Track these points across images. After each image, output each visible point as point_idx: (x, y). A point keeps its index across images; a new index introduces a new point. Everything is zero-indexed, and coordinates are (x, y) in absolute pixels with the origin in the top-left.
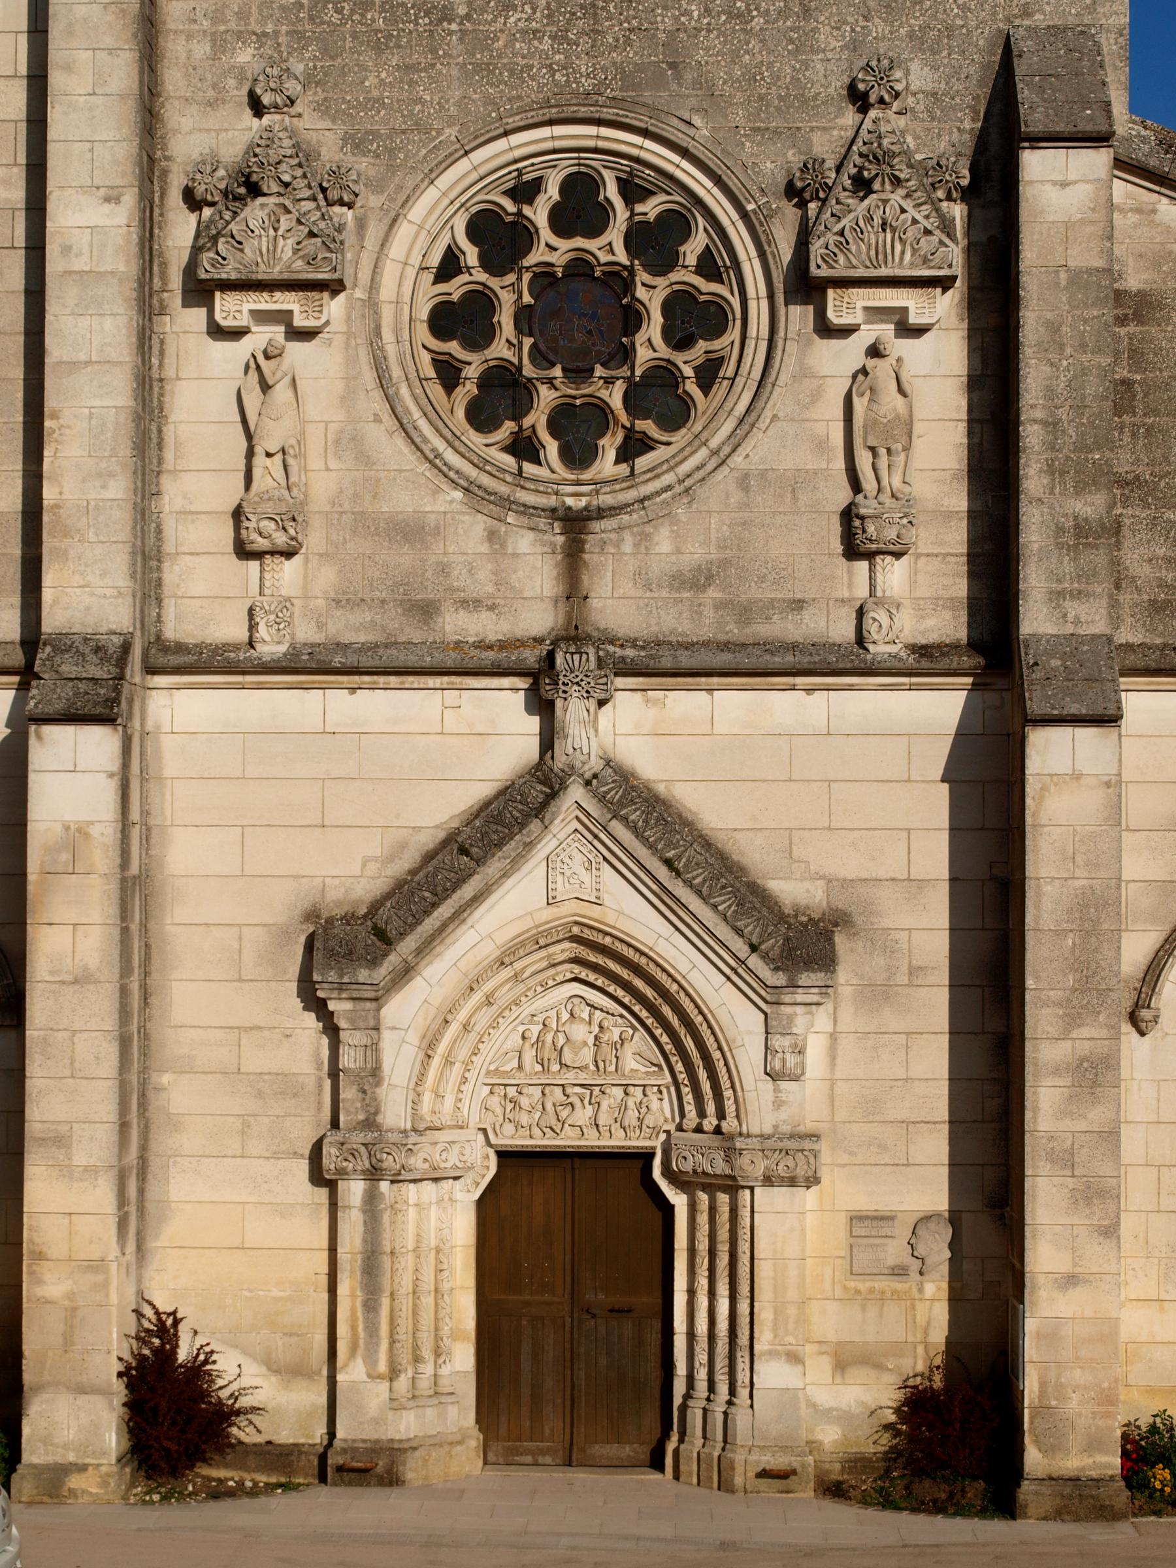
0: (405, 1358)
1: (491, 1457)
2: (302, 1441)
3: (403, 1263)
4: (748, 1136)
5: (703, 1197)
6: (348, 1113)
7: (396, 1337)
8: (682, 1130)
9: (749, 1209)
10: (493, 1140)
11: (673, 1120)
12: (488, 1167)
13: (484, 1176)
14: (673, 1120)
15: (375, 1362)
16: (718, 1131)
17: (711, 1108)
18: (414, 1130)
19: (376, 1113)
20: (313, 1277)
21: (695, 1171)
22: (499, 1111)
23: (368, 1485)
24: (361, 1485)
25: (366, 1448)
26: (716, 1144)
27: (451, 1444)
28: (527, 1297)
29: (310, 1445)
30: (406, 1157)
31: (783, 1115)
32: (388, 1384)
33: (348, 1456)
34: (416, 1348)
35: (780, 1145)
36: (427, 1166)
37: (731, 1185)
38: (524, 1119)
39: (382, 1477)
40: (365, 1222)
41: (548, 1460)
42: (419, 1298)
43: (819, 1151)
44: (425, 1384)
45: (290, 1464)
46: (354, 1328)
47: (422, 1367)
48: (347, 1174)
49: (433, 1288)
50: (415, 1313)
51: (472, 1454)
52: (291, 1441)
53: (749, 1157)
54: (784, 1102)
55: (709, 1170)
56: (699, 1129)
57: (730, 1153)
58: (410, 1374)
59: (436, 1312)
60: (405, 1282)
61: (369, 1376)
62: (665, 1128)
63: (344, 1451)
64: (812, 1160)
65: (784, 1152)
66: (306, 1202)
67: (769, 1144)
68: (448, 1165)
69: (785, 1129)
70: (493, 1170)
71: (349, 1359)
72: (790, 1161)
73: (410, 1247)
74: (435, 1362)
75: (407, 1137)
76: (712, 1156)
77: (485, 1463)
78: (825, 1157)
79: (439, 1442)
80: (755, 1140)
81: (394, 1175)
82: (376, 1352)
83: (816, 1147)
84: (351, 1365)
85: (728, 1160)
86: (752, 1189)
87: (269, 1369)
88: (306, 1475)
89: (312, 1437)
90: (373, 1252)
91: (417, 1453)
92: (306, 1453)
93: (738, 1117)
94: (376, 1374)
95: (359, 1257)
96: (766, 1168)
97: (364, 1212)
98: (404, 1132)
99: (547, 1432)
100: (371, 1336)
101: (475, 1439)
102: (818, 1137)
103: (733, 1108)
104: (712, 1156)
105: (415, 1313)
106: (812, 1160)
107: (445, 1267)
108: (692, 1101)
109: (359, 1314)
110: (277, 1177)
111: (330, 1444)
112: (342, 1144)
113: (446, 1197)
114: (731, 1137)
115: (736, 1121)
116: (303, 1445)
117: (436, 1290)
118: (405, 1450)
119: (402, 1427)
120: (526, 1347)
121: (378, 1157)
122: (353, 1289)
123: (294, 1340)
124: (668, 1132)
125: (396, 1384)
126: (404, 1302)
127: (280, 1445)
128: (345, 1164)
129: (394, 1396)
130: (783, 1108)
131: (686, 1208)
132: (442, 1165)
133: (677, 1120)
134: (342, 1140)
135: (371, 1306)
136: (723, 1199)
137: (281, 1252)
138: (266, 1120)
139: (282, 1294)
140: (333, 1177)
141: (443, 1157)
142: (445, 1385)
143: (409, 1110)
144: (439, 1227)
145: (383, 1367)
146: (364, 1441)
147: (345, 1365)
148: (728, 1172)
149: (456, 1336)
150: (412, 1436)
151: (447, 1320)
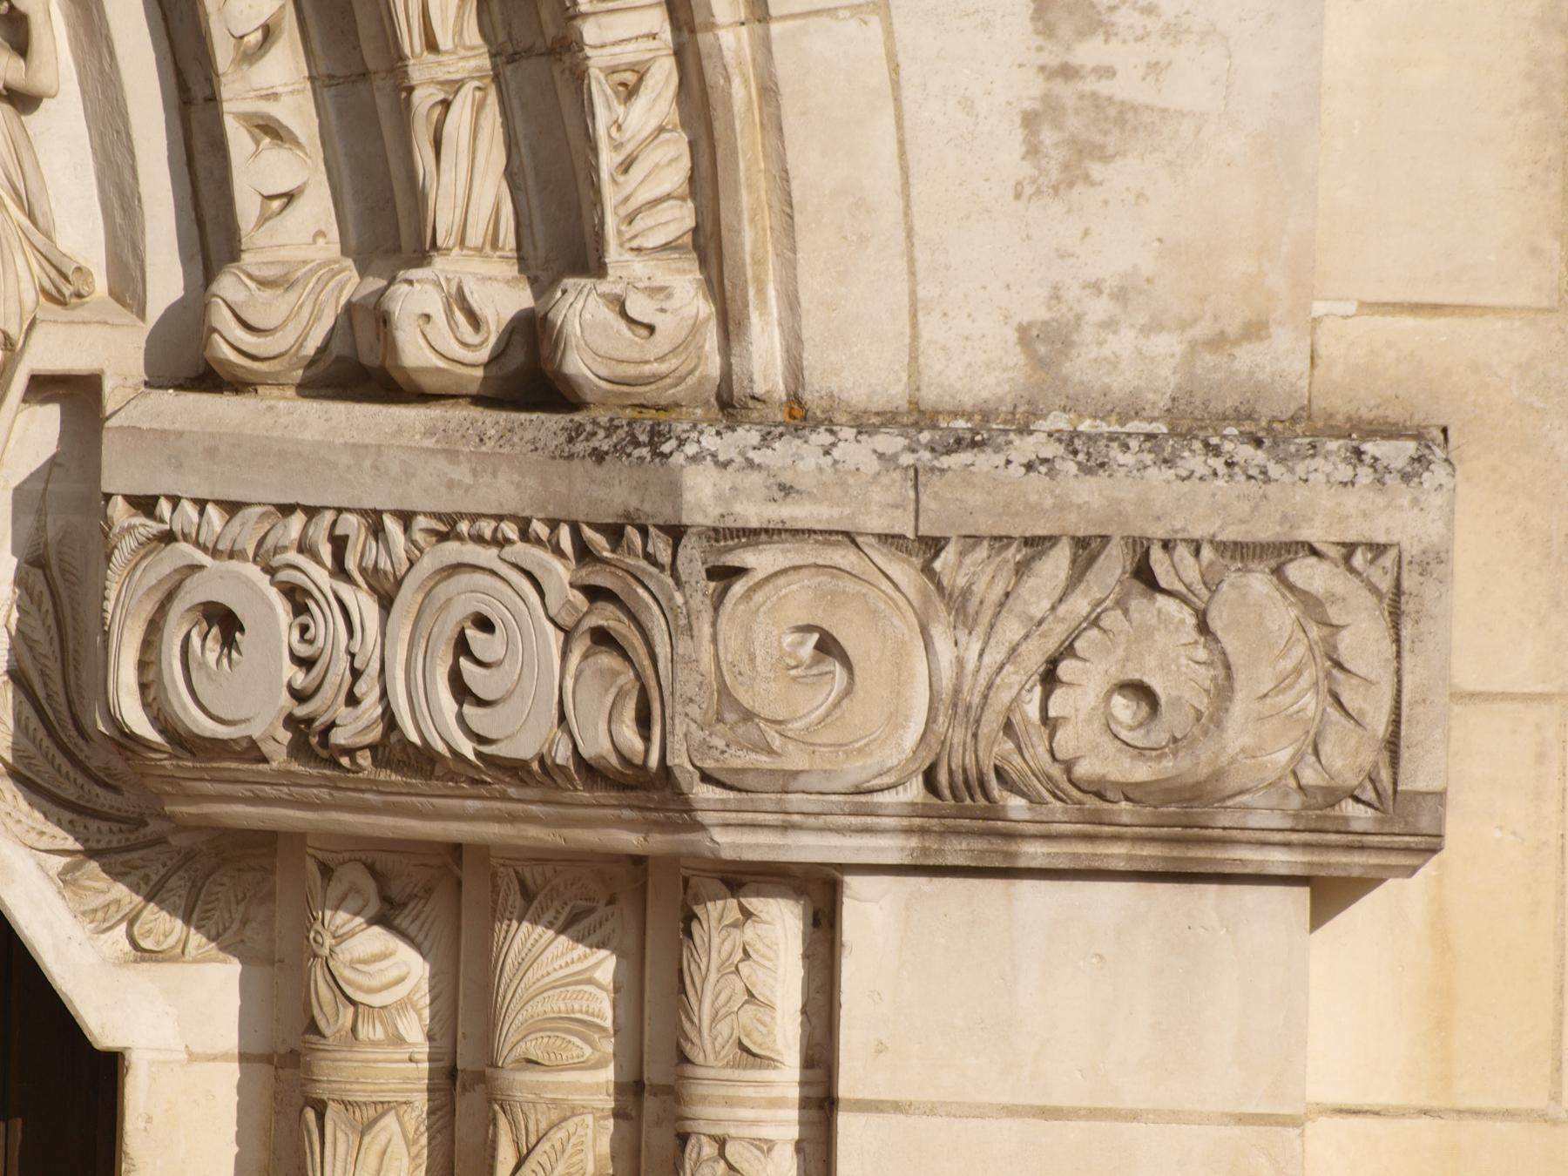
4: (799, 416)
5: (385, 973)
8: (209, 378)
9: (787, 1078)
11: (128, 285)
14: (128, 285)
16: (528, 374)
17: (468, 176)
21: (310, 739)
26: (502, 490)
31: (1118, 230)
35: (1085, 498)
37: (642, 867)
43: (1434, 561)
53: (797, 601)
54: (1124, 116)
55: (438, 722)
56: (358, 369)
57: (629, 570)
62: (57, 349)
64: (1363, 638)
65: (1113, 566)
67: (979, 489)
69: (1135, 359)
72: (1162, 643)
76: (466, 596)
78: (1484, 626)
80: (856, 452)
83: (1401, 520)
85: (607, 626)
86: (820, 893)
93: (708, 247)
96: (952, 705)
102: (1429, 442)
103: (667, 165)
104: (466, 596)
106: (1363, 638)
108: (299, 112)
114: (646, 427)
115: (688, 297)
124: (75, 394)
130: (1117, 176)
131: (222, 1088)
133: (166, 282)
136: (563, 980)
148: (606, 733)
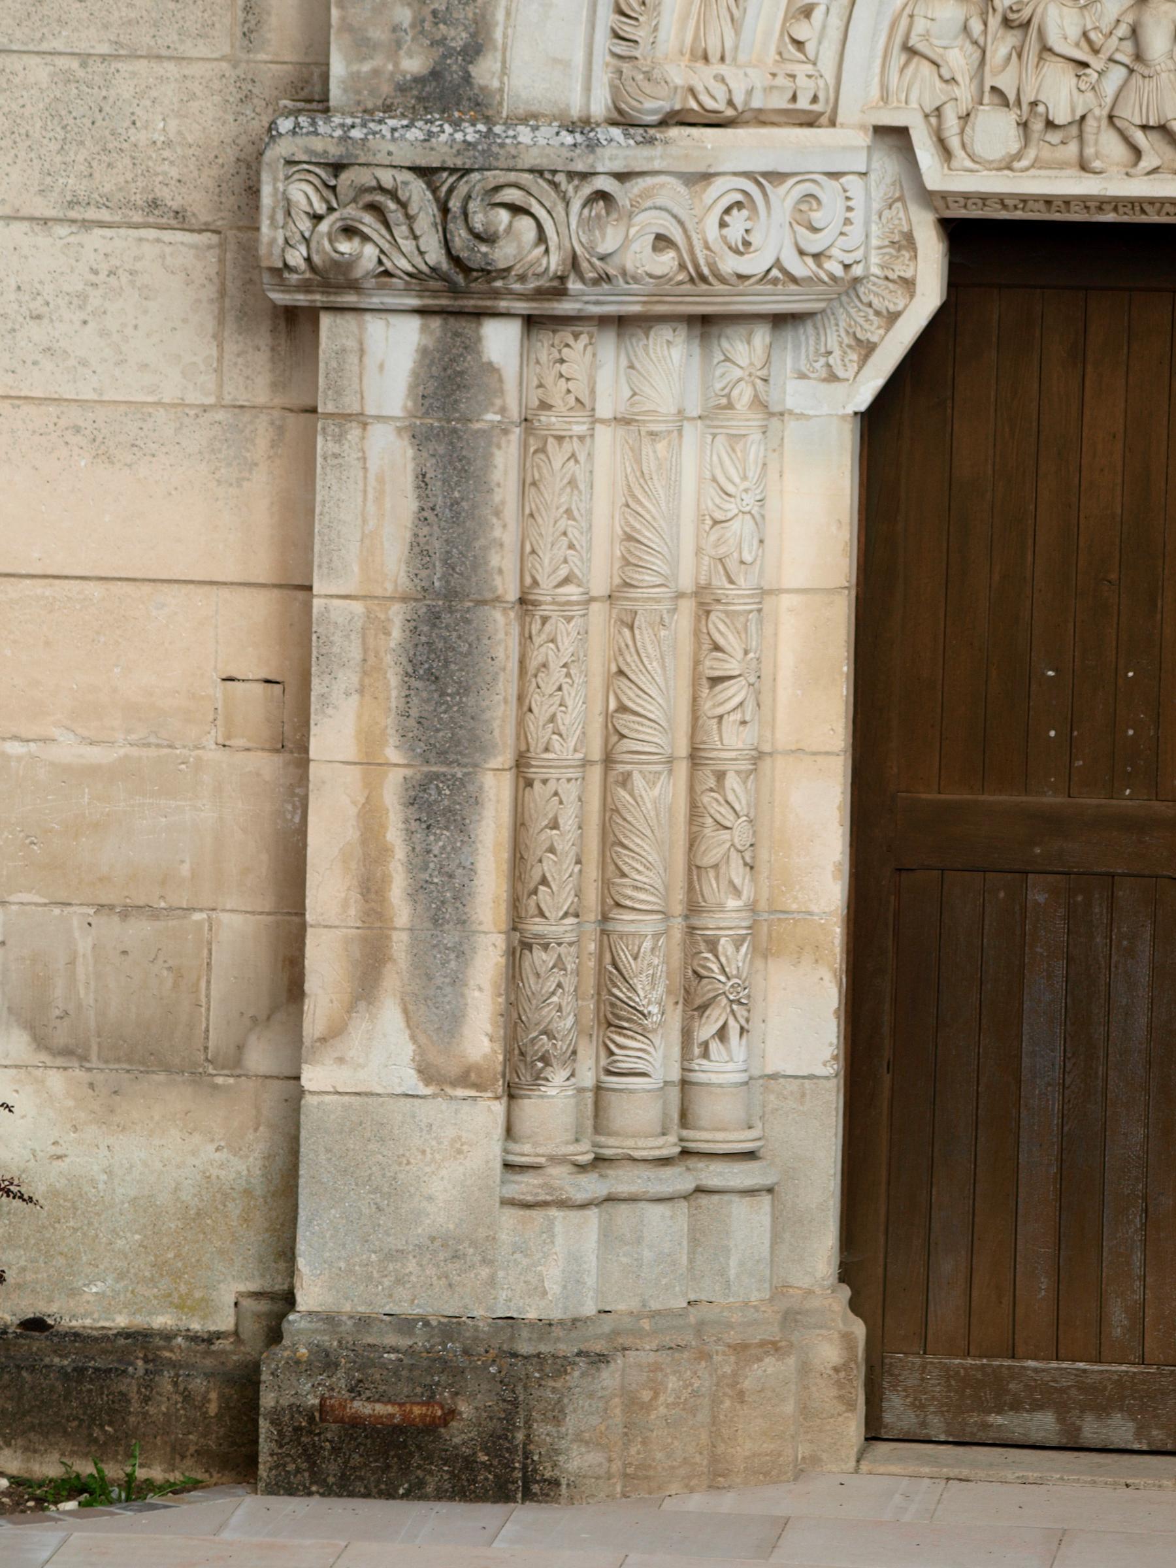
0: (563, 1008)
1: (898, 1411)
2: (162, 1320)
3: (567, 645)
6: (362, 46)
7: (536, 926)
10: (934, 174)
12: (909, 284)
13: (893, 317)
15: (451, 1023)
18: (623, 120)
19: (474, 50)
20: (220, 691)
22: (959, 59)
23: (416, 1492)
24: (390, 1495)
25: (410, 1351)
27: (740, 1349)
28: (1051, 799)
29: (194, 1338)
30: (587, 224)
32: (499, 1108)
33: (340, 1380)
34: (611, 972)
36: (666, 262)
38: (1060, 93)
39: (469, 1463)
40: (422, 479)
41: (1121, 1430)
42: (625, 781)
44: (640, 1117)
45: (117, 1410)
46: (371, 889)
47: (631, 1051)
48: (354, 286)
49: (683, 750)
50: (611, 840)
51: (825, 1394)
52: (121, 1321)
58: (587, 1078)
59: (693, 842)
60: (571, 719)
61: (426, 1073)
63: (326, 1361)
66: (194, 397)
68: (754, 264)
70: (930, 295)
71: (351, 1008)
73: (599, 587)
74: (687, 1035)
75: (592, 146)
77: (874, 1433)
79: (689, 1336)
81: (540, 294)
82: (457, 981)
84: (359, 1028)
87: (41, 1042)
88: (177, 1452)
89: (205, 1306)
90: (451, 595)
91: (609, 1378)
92: (173, 1365)
94: (454, 1070)
95: (397, 615)
97: (420, 438)
98: (582, 125)
99: (1118, 1318)
100: (437, 921)
101: (835, 1337)
105: (611, 840)
107: (732, 666)
109: (394, 835)
110: (83, 297)
111: (274, 1335)
112: (337, 168)
113: (743, 396)
116: (168, 1336)
117: (695, 757)
118: (561, 1366)
119: (553, 1276)
120: (1043, 994)
121: (478, 221)
122: (369, 740)
123: (139, 930)
125: (530, 1109)
126: (570, 792)
127: (76, 1335)
128: (345, 247)
129: (525, 1152)
132: (730, 264)
134: (335, 152)
135: (438, 805)
137: (96, 590)
138: (39, 71)
139: (95, 755)
140: (301, 299)
141: (735, 232)
142: (721, 1123)
143: (602, 38)
144: (720, 523)
145: (480, 1040)
146: (405, 1324)
147: (336, 1032)
149: (766, 935)
150: (589, 1309)
151: (737, 872)
